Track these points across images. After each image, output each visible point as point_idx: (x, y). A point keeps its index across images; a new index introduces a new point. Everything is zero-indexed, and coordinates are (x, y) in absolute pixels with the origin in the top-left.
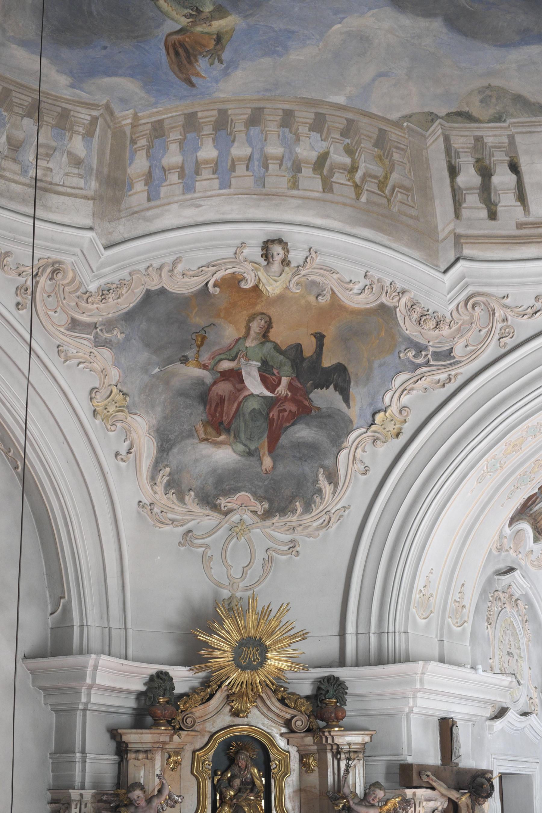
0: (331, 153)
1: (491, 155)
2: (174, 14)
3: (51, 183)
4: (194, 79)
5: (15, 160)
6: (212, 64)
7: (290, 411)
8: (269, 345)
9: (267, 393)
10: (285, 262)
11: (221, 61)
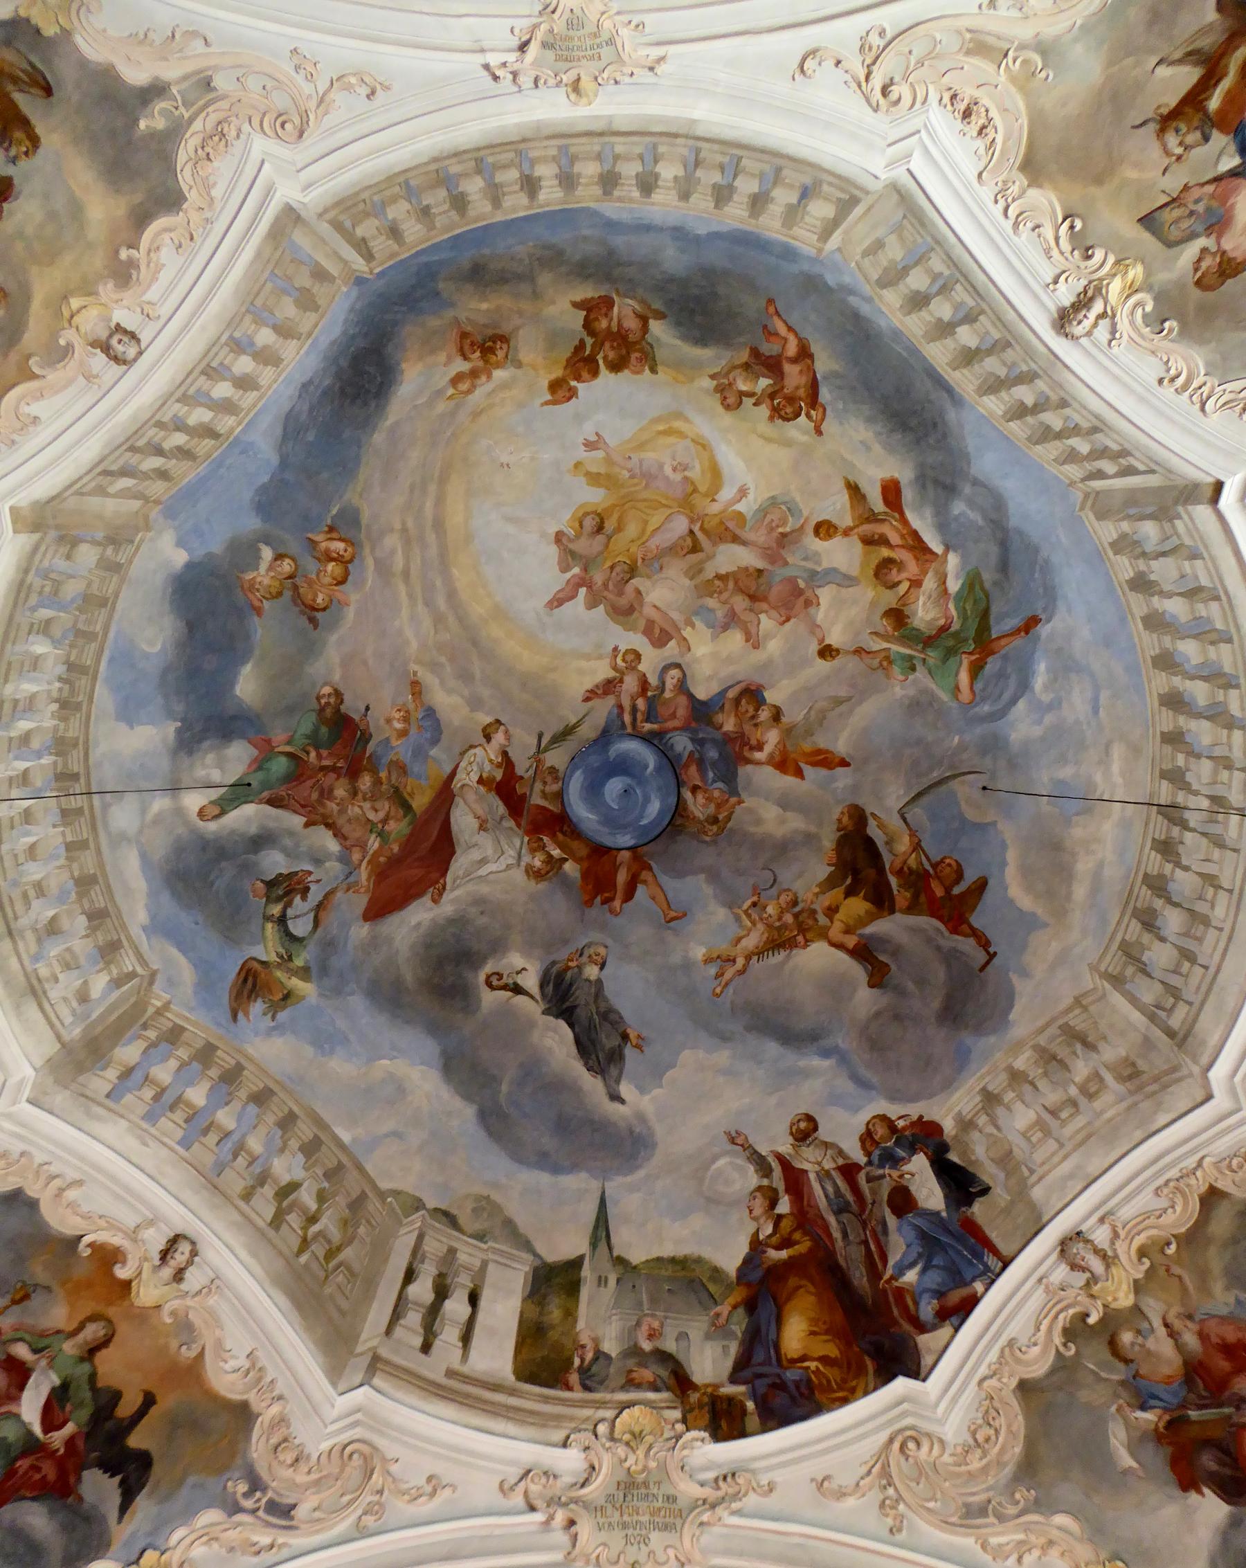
0: (303, 1188)
1: (456, 1275)
2: (270, 944)
3: (45, 992)
4: (240, 1015)
5: (39, 941)
6: (265, 1014)
7: (44, 1477)
8: (86, 1368)
9: (37, 1430)
10: (179, 1276)
11: (273, 1018)
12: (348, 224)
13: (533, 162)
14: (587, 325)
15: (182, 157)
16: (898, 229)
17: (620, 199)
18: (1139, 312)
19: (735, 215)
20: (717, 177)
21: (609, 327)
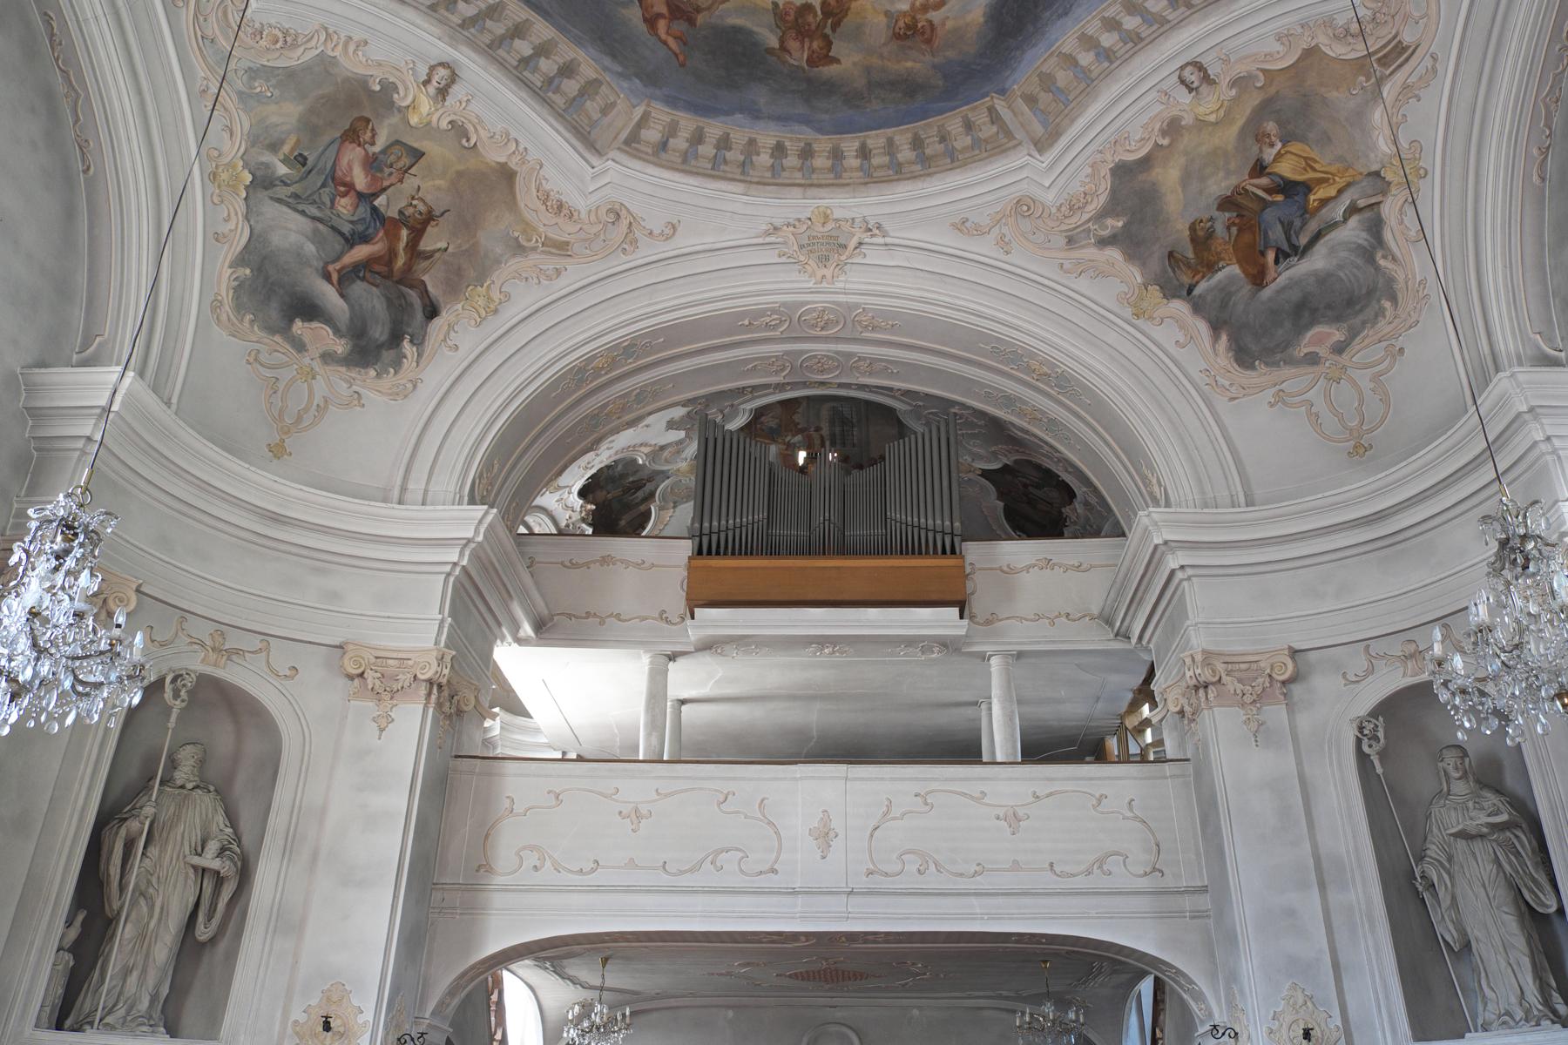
12: (1001, 136)
13: (861, 168)
14: (829, 44)
15: (1103, 198)
16: (593, 124)
17: (799, 140)
18: (402, 93)
19: (714, 129)
20: (729, 155)
21: (811, 43)
